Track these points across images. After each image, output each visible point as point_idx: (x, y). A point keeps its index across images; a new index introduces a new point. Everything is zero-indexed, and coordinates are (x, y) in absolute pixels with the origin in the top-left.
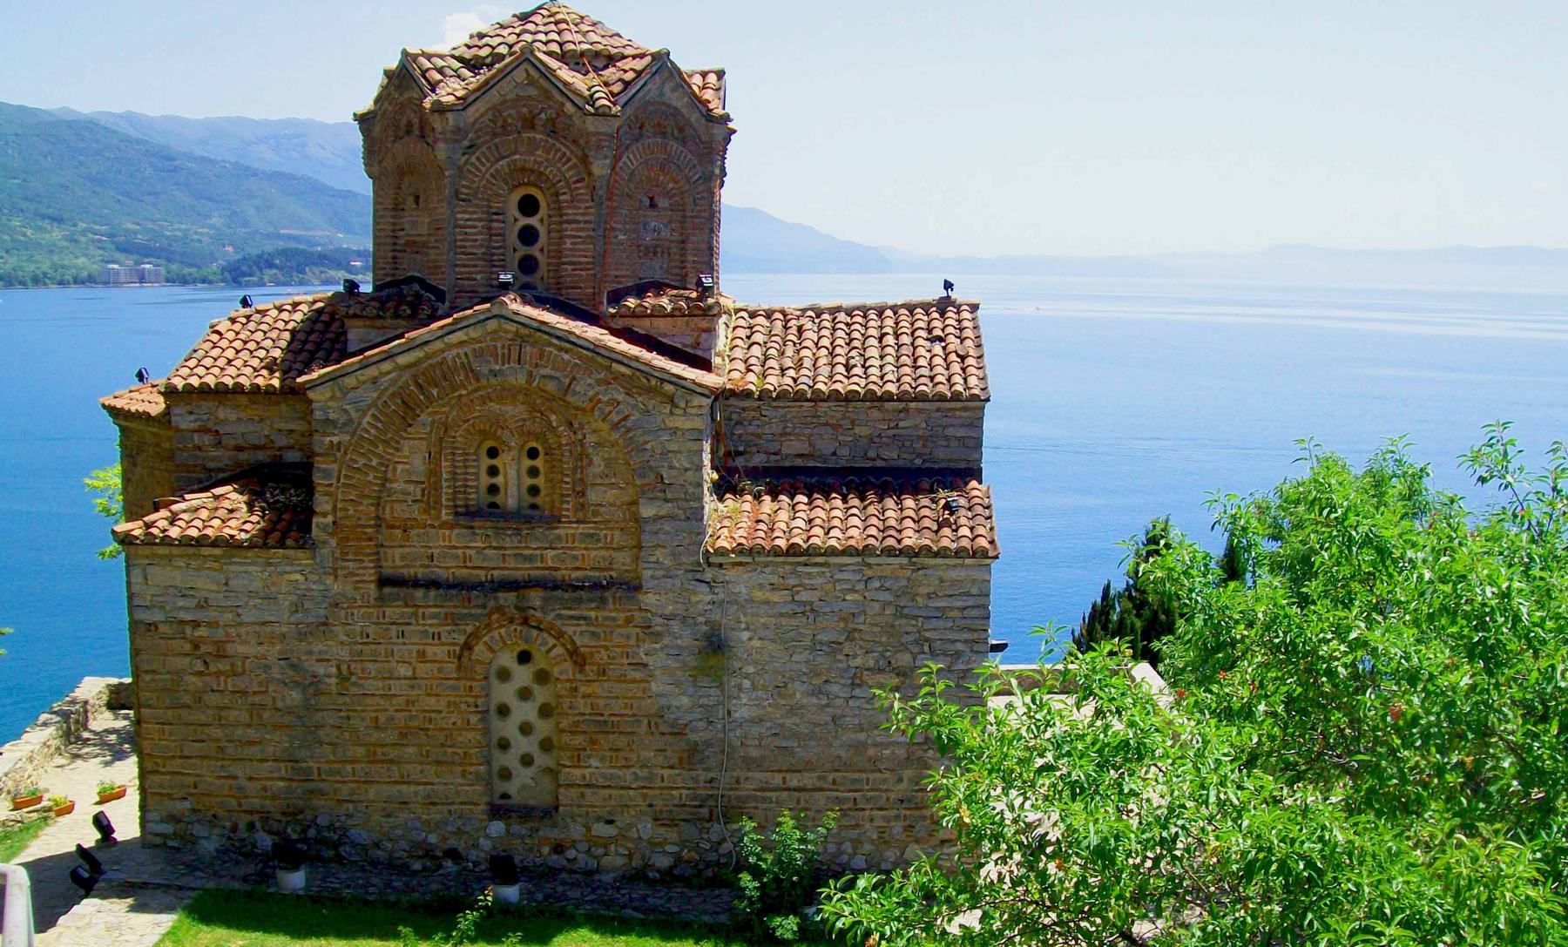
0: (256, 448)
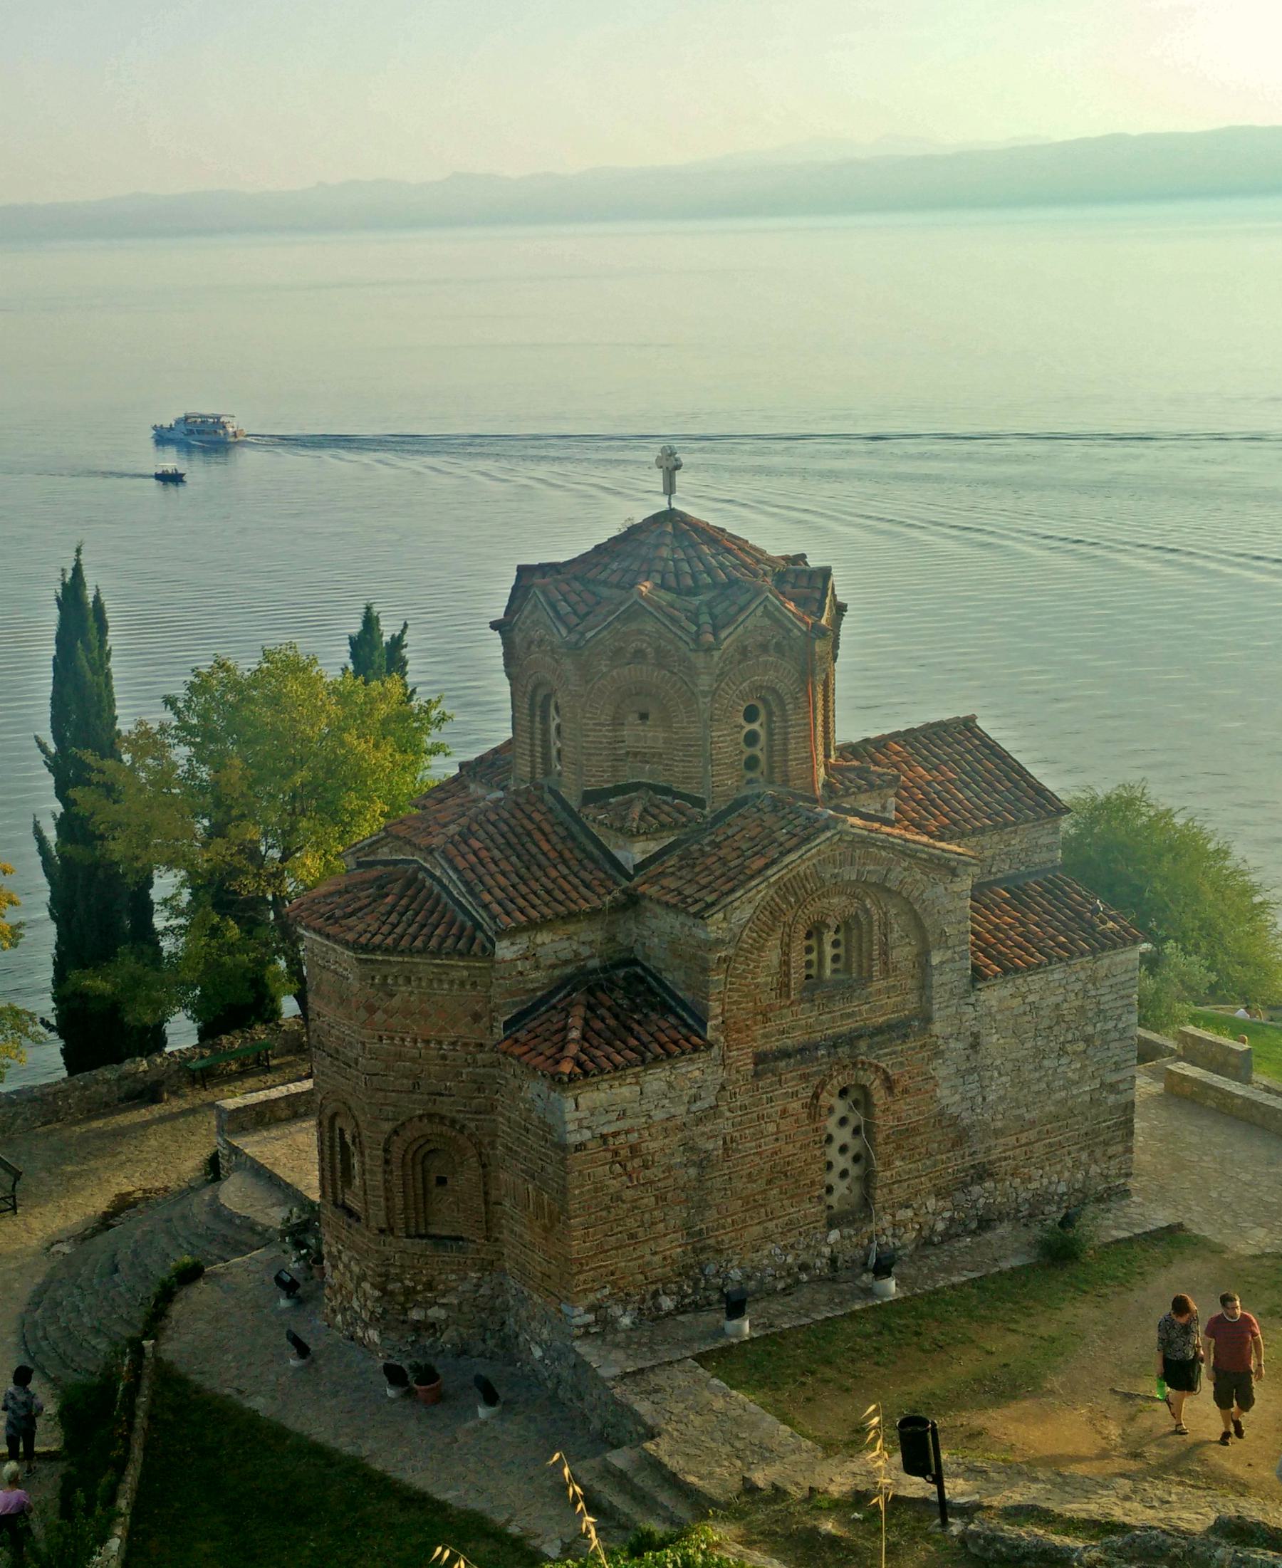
0: (566, 962)
